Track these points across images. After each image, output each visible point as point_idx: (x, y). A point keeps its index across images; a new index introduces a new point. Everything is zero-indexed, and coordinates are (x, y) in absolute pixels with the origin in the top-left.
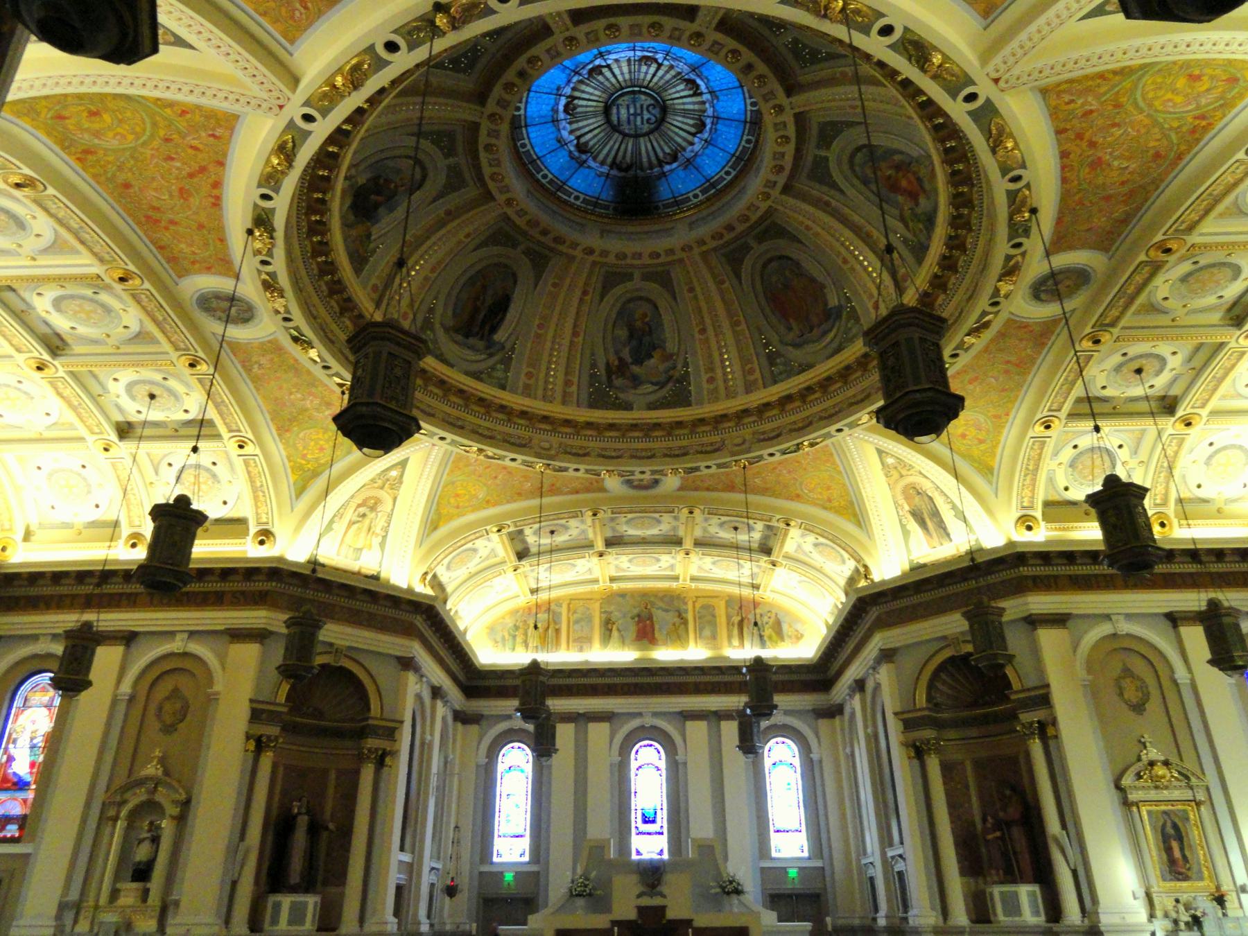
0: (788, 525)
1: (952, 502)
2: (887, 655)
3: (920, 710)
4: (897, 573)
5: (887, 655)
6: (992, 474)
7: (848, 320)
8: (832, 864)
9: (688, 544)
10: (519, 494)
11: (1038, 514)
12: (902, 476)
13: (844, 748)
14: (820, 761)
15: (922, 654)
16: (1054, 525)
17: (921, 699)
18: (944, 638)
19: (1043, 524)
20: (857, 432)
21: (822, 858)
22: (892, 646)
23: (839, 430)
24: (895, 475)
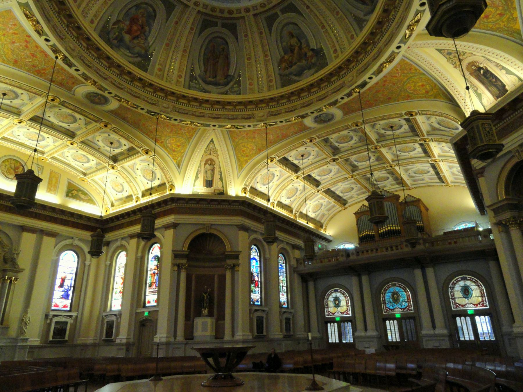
0: (147, 153)
1: (221, 173)
2: (174, 226)
3: (184, 251)
4: (191, 193)
5: (174, 226)
6: (242, 169)
7: (235, 84)
8: (82, 314)
9: (77, 140)
10: (16, 62)
11: (248, 189)
12: (210, 154)
13: (106, 261)
14: (89, 266)
15: (192, 229)
16: (251, 195)
17: (186, 248)
18: (204, 224)
19: (248, 193)
20: (218, 130)
21: (78, 311)
22: (178, 222)
23: (214, 126)
24: (208, 152)
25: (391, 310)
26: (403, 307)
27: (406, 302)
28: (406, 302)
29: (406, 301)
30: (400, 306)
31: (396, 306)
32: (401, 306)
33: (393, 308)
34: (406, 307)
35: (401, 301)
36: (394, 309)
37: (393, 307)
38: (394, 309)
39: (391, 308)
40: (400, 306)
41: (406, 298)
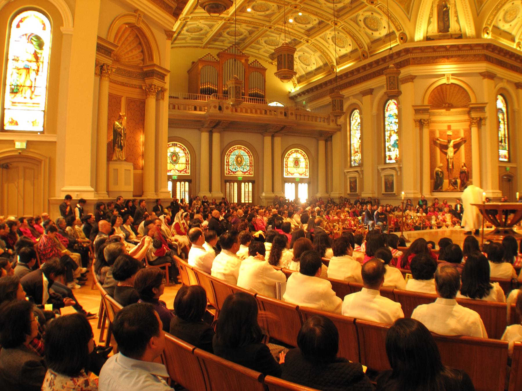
25: (234, 172)
26: (245, 170)
27: (248, 166)
28: (248, 166)
29: (249, 165)
30: (242, 170)
31: (239, 169)
32: (243, 170)
33: (235, 171)
34: (247, 172)
35: (244, 165)
36: (236, 172)
37: (235, 169)
38: (236, 172)
39: (234, 170)
40: (242, 170)
41: (249, 163)
